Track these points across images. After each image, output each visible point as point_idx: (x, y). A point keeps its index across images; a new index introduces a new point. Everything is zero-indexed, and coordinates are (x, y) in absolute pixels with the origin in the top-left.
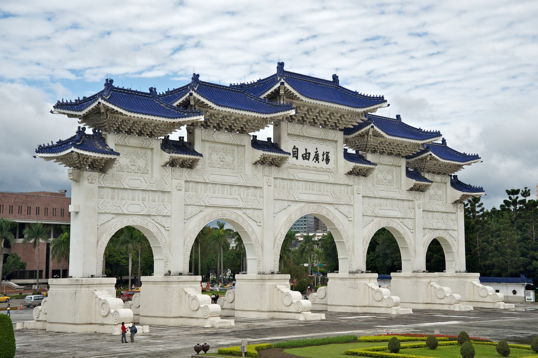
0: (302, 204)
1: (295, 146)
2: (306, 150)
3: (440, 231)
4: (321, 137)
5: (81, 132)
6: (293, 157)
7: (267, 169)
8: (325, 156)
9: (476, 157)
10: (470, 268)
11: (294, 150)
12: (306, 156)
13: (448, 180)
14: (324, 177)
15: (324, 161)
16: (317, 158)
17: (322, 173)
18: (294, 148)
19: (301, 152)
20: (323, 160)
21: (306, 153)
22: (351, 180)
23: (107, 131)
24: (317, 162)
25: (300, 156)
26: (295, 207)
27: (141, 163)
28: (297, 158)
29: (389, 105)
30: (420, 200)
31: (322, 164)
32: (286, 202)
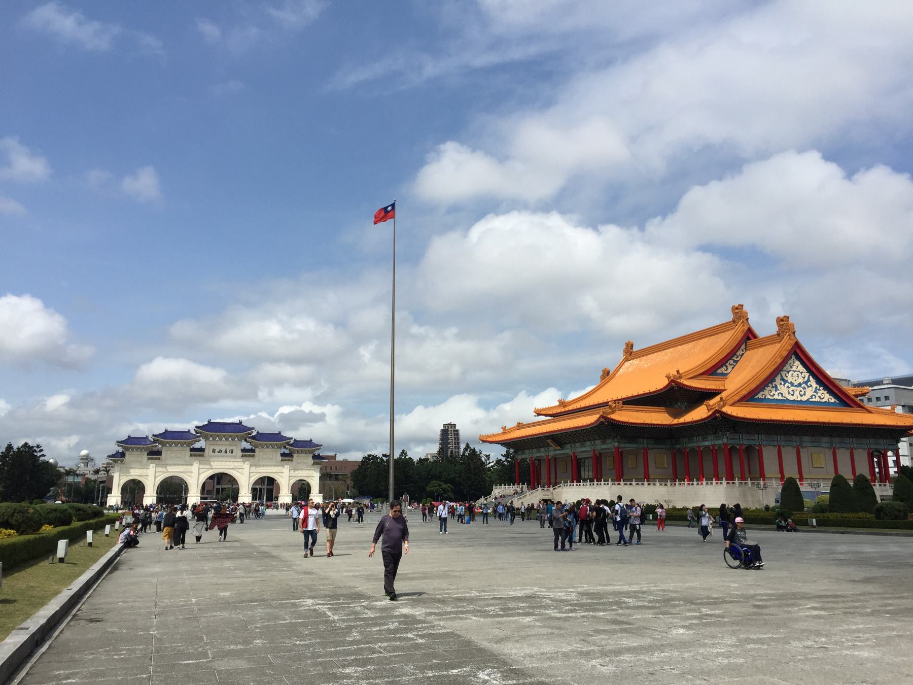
10: (320, 492)
12: (220, 452)
31: (229, 454)
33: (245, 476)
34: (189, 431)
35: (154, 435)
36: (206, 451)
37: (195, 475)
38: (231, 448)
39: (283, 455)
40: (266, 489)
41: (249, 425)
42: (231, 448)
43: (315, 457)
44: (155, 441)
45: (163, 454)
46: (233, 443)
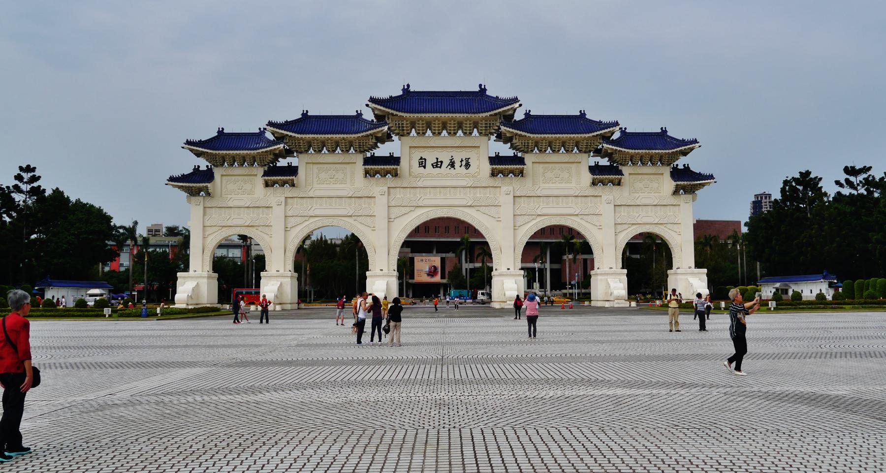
3: (648, 226)
5: (197, 170)
8: (464, 163)
9: (695, 141)
10: (698, 265)
12: (437, 164)
13: (667, 171)
14: (464, 183)
15: (463, 167)
16: (452, 164)
18: (421, 158)
19: (430, 161)
23: (217, 166)
25: (429, 165)
26: (419, 212)
27: (248, 186)
28: (425, 167)
29: (520, 105)
30: (609, 194)
31: (459, 170)
33: (506, 224)
34: (359, 115)
35: (270, 124)
36: (404, 163)
37: (381, 222)
38: (464, 154)
39: (595, 170)
40: (558, 259)
41: (504, 95)
42: (464, 154)
43: (676, 174)
44: (280, 139)
45: (301, 171)
46: (468, 141)
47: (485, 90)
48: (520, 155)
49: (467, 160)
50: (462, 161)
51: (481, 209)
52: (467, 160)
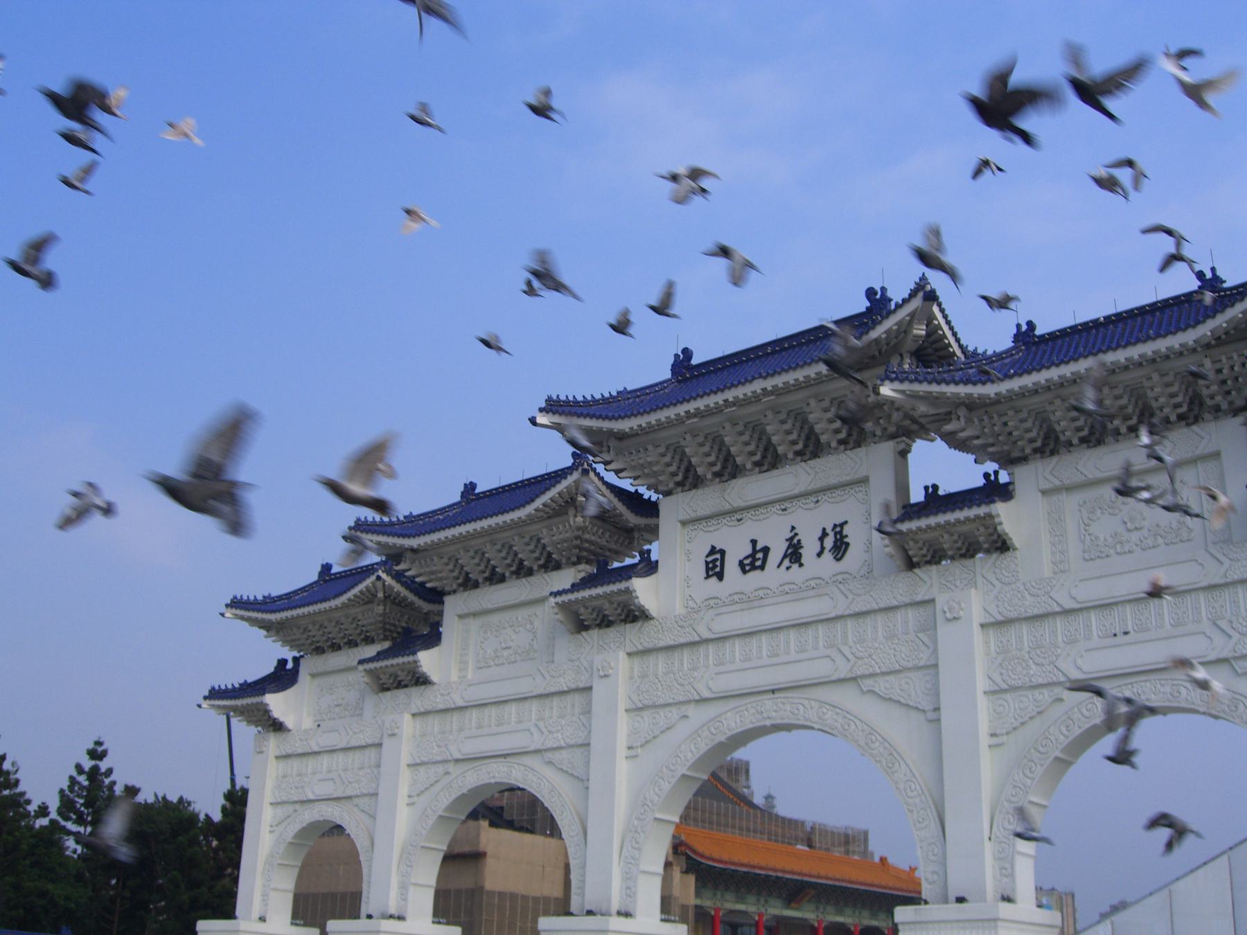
0: (733, 703)
1: (713, 548)
2: (754, 542)
4: (796, 491)
6: (708, 577)
7: (611, 633)
8: (829, 542)
11: (709, 559)
12: (755, 560)
15: (827, 556)
16: (794, 553)
17: (811, 593)
18: (713, 550)
20: (819, 555)
21: (755, 551)
22: (930, 581)
24: (795, 566)
25: (731, 567)
28: (720, 576)
32: (674, 709)
47: (885, 300)
48: (1004, 477)
49: (839, 528)
50: (824, 534)
51: (881, 685)
52: (839, 528)
